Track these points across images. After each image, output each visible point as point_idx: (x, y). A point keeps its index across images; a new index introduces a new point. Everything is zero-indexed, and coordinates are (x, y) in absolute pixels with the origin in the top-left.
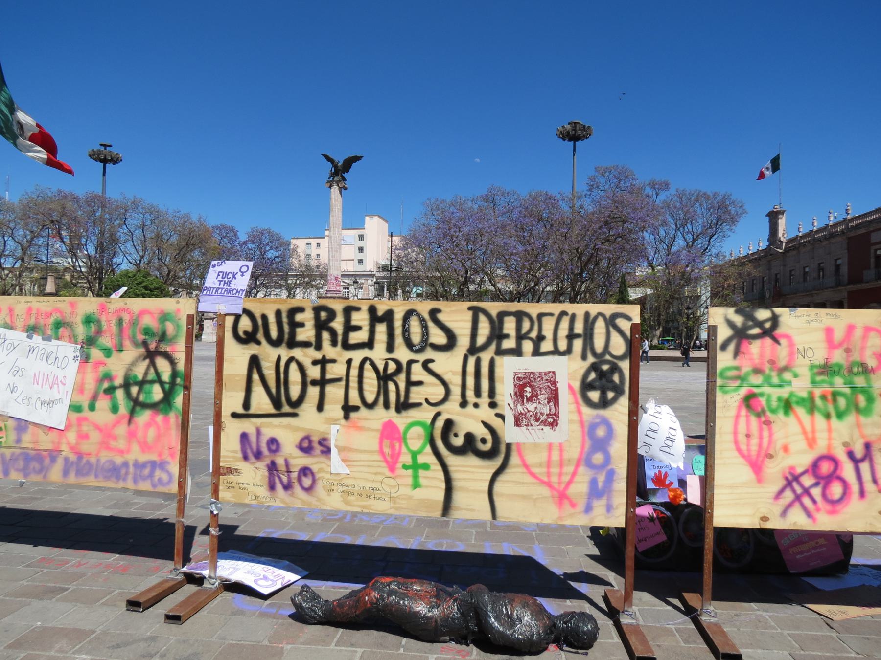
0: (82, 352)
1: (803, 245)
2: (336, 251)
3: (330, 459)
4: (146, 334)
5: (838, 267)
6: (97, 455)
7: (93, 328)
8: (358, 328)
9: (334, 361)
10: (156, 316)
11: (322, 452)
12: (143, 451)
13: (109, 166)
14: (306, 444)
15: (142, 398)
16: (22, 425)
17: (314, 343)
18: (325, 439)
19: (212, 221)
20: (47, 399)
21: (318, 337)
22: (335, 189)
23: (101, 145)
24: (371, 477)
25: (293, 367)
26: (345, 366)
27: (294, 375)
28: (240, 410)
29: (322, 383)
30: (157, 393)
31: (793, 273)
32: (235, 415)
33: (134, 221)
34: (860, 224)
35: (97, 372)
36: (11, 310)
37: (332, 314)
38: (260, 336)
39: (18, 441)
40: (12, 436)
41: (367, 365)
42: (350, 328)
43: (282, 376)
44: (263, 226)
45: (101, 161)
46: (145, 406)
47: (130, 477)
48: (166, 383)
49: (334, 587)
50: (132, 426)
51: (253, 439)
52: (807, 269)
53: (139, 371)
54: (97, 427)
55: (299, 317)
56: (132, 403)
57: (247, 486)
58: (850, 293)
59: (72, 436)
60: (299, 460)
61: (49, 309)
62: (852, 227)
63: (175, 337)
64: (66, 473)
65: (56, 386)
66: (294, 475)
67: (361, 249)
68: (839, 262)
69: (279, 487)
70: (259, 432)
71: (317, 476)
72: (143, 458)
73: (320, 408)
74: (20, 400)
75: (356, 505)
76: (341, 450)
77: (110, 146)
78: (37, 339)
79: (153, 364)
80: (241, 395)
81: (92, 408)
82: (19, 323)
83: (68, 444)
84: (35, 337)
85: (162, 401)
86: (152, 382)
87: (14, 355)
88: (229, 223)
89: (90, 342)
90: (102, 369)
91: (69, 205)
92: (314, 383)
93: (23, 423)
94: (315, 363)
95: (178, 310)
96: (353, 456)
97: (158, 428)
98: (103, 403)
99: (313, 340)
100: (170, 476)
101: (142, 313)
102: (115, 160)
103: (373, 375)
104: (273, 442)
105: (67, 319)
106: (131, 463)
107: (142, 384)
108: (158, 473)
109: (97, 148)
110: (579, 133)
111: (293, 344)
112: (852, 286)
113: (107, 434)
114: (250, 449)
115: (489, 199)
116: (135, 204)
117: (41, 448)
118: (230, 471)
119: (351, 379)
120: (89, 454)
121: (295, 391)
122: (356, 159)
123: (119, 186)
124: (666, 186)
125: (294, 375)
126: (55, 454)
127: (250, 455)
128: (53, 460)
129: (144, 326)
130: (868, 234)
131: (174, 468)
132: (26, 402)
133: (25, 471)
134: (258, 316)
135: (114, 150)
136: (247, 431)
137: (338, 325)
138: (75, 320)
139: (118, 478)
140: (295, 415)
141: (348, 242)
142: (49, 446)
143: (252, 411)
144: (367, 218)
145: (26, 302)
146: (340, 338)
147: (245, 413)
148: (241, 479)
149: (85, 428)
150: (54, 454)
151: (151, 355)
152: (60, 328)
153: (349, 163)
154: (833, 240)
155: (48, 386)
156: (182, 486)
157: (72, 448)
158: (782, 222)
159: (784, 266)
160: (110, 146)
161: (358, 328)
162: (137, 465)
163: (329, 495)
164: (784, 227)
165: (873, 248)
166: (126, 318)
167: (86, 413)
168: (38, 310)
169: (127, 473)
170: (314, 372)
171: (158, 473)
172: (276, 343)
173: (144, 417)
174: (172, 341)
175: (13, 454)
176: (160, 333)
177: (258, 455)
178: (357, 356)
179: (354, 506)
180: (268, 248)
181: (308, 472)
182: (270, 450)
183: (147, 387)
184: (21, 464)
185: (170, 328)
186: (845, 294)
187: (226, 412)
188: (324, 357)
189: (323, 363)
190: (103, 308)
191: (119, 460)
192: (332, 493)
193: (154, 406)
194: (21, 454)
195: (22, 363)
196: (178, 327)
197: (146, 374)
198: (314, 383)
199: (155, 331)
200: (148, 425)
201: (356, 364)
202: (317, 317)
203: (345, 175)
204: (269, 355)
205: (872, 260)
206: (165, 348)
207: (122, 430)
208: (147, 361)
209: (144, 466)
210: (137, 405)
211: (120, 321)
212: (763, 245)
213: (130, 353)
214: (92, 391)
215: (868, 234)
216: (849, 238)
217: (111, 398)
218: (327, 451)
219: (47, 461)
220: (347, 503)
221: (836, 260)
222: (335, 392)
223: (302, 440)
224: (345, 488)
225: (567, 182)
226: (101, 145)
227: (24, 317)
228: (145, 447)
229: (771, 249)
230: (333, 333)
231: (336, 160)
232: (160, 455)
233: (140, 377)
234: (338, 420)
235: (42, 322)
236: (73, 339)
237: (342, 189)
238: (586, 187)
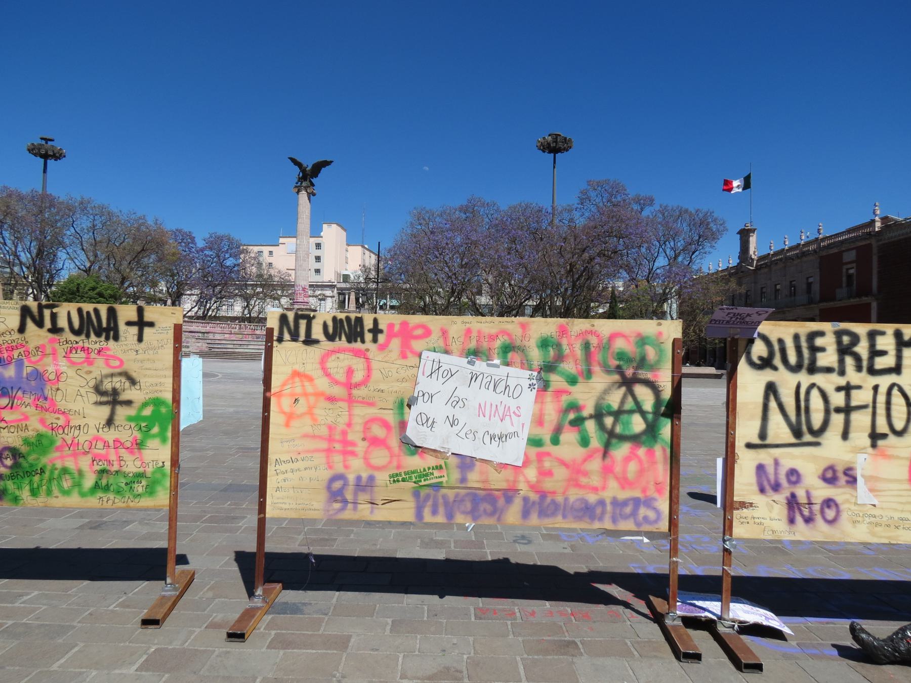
0: (540, 379)
1: (776, 263)
2: (304, 261)
3: (856, 489)
4: (620, 359)
5: (809, 285)
6: (564, 493)
7: (552, 352)
8: (883, 353)
9: (859, 387)
10: (632, 339)
11: (848, 482)
12: (623, 488)
13: (51, 162)
14: (829, 475)
15: (618, 429)
16: (466, 463)
17: (837, 369)
18: (850, 469)
19: (170, 225)
20: (498, 432)
21: (841, 362)
23: (42, 139)
24: (900, 507)
25: (815, 393)
26: (871, 393)
27: (816, 402)
28: (756, 440)
29: (847, 410)
30: (637, 424)
31: (764, 290)
32: (749, 446)
33: (84, 223)
34: (831, 244)
35: (559, 401)
36: (444, 333)
37: (855, 339)
38: (777, 361)
39: (463, 480)
40: (455, 475)
41: (895, 391)
42: (875, 353)
43: (803, 404)
44: (221, 232)
45: (42, 156)
46: (623, 438)
47: (607, 517)
48: (648, 413)
49: (820, 623)
50: (608, 461)
51: (770, 470)
52: (778, 287)
53: (615, 399)
54: (563, 463)
55: (819, 342)
56: (606, 436)
57: (763, 521)
58: (821, 310)
59: (531, 473)
60: (822, 492)
61: (494, 331)
62: (824, 247)
63: (658, 362)
64: (526, 514)
65: (507, 418)
66: (816, 508)
67: (318, 259)
68: (811, 280)
69: (799, 519)
70: (776, 463)
71: (842, 507)
72: (623, 495)
73: (845, 435)
74: (462, 434)
75: (881, 536)
76: (868, 479)
78: (480, 366)
79: (631, 392)
80: (757, 424)
81: (555, 441)
82: (455, 347)
83: (528, 482)
84: (477, 362)
85: (644, 433)
86: (631, 412)
87: (451, 384)
88: (186, 229)
89: (549, 368)
90: (565, 398)
91: (13, 202)
92: (838, 410)
93: (468, 460)
94: (839, 389)
95: (660, 334)
96: (880, 486)
97: (640, 461)
98: (569, 436)
99: (835, 365)
100: (658, 513)
101: (613, 337)
102: (58, 156)
103: (902, 401)
104: (794, 475)
105: (518, 343)
106: (608, 501)
107: (617, 414)
108: (643, 511)
109: (37, 142)
110: (560, 145)
111: (813, 369)
112: (825, 304)
113: (576, 471)
114: (766, 482)
115: (469, 210)
116: (84, 206)
117: (493, 487)
118: (743, 505)
119: (878, 405)
120: (554, 493)
121: (817, 420)
122: (326, 163)
123: (63, 183)
124: (651, 201)
125: (816, 402)
126: (510, 494)
127: (767, 488)
128: (509, 500)
129: (617, 351)
130: (840, 254)
131: (664, 505)
132: (471, 436)
133: (474, 513)
134: (774, 339)
135: (57, 145)
136: (763, 462)
137: (862, 349)
138: (526, 343)
139: (592, 518)
140: (817, 444)
142: (504, 485)
143: (769, 441)
144: (325, 226)
145: (463, 322)
146: (865, 364)
147: (762, 443)
148: (756, 513)
149: (547, 464)
150: (509, 494)
151: (628, 383)
152: (510, 351)
154: (805, 259)
155: (497, 418)
156: (673, 523)
157: (532, 487)
158: (753, 240)
159: (755, 283)
161: (883, 353)
162: (615, 502)
163: (855, 527)
165: (845, 267)
166: (594, 341)
167: (549, 448)
168: (479, 332)
169: (603, 512)
170: (838, 399)
171: (643, 511)
172: (796, 369)
173: (621, 451)
174: (653, 368)
175: (457, 495)
176: (638, 358)
177: (776, 487)
178: (884, 382)
179: (881, 537)
180: (227, 256)
181: (832, 504)
182: (789, 482)
183: (624, 417)
184: (468, 505)
185: (651, 353)
187: (740, 444)
188: (848, 383)
189: (847, 389)
190: (563, 331)
191: (592, 498)
192: (858, 525)
193: (635, 439)
194: (468, 494)
195: (462, 392)
196: (660, 352)
197: (623, 402)
198: (838, 410)
199: (631, 356)
200: (627, 460)
201: (883, 390)
202: (839, 342)
203: (314, 180)
204: (787, 382)
205: (844, 279)
206: (644, 374)
207: (595, 465)
208: (623, 389)
209: (625, 503)
210: (611, 437)
211: (587, 346)
212: (734, 262)
213: (601, 381)
214: (555, 422)
215: (840, 254)
216: (821, 258)
217: (579, 431)
218: (853, 481)
219: (501, 502)
220: (873, 534)
221: (808, 278)
222: (861, 420)
223: (826, 470)
224: (872, 519)
225: (559, 195)
226: (42, 139)
227: (462, 340)
228: (625, 483)
229: (742, 266)
230: (858, 358)
232: (644, 491)
233: (615, 406)
234: (865, 448)
235: (485, 345)
236: (526, 364)
237: (311, 195)
238: (577, 201)
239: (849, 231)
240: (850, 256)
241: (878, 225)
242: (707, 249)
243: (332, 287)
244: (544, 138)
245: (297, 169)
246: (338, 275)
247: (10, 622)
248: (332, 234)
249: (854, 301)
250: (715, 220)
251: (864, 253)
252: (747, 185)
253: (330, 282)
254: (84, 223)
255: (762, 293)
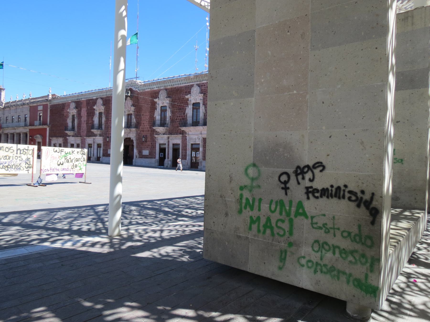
1: (12, 106)
5: (26, 118)
34: (34, 102)
52: (14, 117)
58: (30, 130)
62: (32, 102)
68: (26, 116)
130: (37, 107)
154: (24, 106)
159: (4, 114)
164: (4, 96)
165: (39, 112)
186: (28, 130)
205: (38, 117)
215: (37, 107)
239: (42, 97)
240: (40, 108)
241: (50, 97)
249: (41, 127)
251: (45, 107)
255: (7, 119)
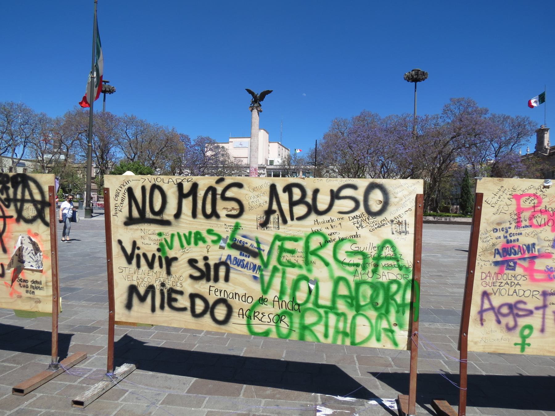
2: (256, 152)
13: (107, 95)
19: (179, 131)
22: (255, 112)
77: (108, 82)
88: (185, 133)
102: (111, 91)
110: (420, 77)
122: (268, 92)
135: (111, 85)
141: (244, 146)
153: (264, 94)
158: (547, 136)
160: (108, 82)
164: (548, 139)
225: (430, 108)
231: (256, 94)
237: (259, 112)
242: (522, 143)
243: (264, 168)
244: (409, 73)
245: (251, 97)
246: (266, 160)
247: (94, 369)
248: (262, 136)
250: (529, 123)
252: (542, 99)
253: (261, 165)
254: (131, 132)
